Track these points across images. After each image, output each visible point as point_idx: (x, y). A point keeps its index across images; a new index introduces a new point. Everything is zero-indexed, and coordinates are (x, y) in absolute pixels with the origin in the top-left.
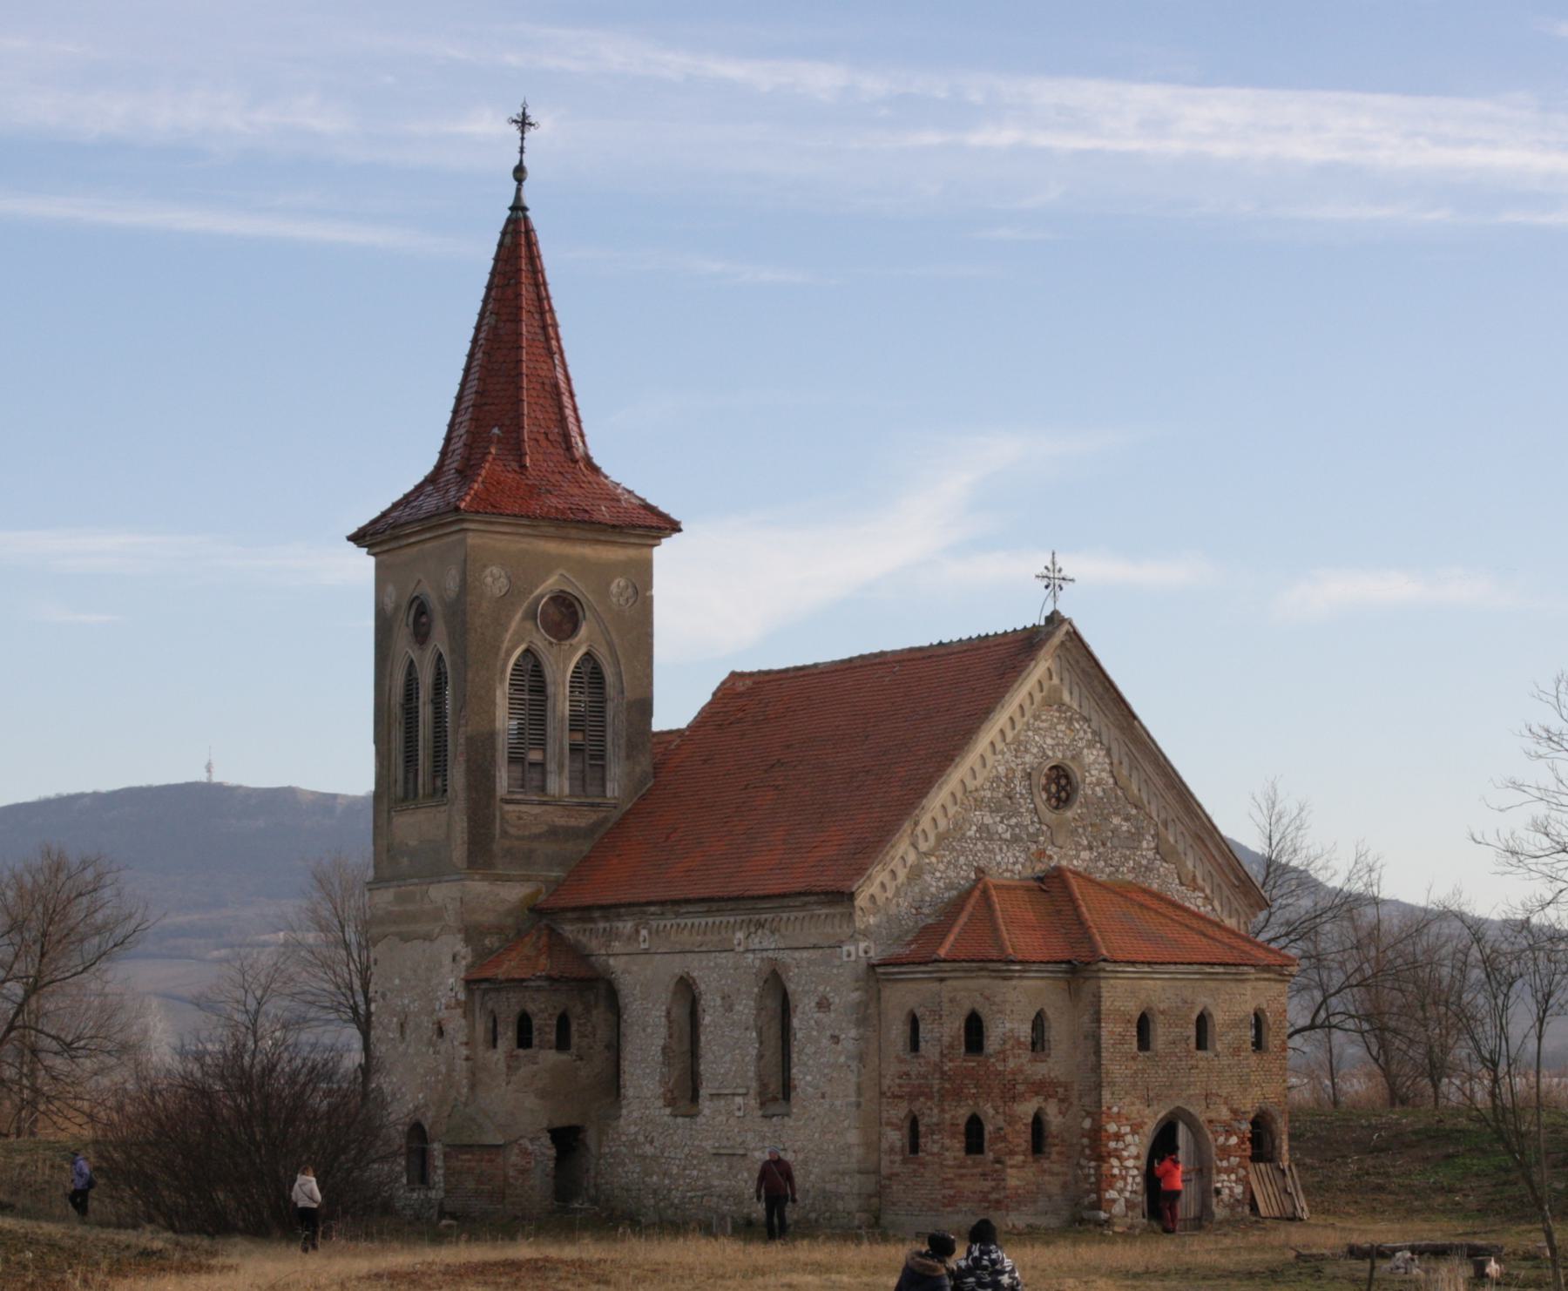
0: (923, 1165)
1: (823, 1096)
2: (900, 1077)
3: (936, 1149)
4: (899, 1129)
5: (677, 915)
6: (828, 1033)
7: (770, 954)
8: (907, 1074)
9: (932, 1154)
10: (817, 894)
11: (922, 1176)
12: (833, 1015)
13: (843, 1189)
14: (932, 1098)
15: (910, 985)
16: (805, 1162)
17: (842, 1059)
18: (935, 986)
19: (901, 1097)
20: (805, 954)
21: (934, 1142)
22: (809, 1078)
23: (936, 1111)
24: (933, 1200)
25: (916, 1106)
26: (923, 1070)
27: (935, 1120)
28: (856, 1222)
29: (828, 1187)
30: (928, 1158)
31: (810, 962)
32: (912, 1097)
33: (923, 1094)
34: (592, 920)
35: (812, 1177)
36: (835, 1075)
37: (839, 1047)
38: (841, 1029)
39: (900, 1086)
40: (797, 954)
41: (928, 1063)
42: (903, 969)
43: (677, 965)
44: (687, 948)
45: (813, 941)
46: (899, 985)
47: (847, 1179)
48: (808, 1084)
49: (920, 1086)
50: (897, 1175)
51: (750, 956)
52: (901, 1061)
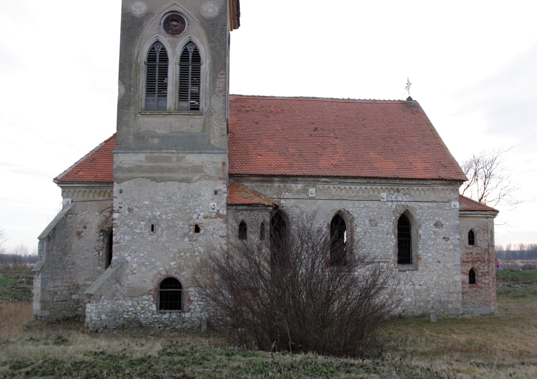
0: (481, 288)
1: (439, 262)
2: (468, 254)
3: (487, 282)
4: (467, 274)
5: (340, 183)
6: (442, 237)
7: (403, 203)
8: (471, 253)
9: (485, 284)
10: (443, 179)
11: (480, 292)
12: (444, 229)
13: (451, 299)
14: (484, 262)
15: (472, 219)
16: (427, 289)
17: (451, 247)
18: (485, 220)
19: (468, 262)
20: (426, 204)
21: (486, 279)
22: (430, 255)
23: (486, 267)
24: (485, 301)
25: (476, 266)
26: (479, 252)
27: (486, 271)
28: (461, 312)
29: (442, 299)
30: (483, 285)
31: (429, 208)
32: (473, 262)
33: (479, 261)
34: (272, 182)
35: (432, 295)
36: (446, 253)
37: (449, 242)
38: (451, 236)
39: (467, 258)
40: (421, 204)
41: (482, 249)
42: (473, 213)
43: (337, 206)
44: (345, 198)
45: (431, 199)
46: (467, 219)
47: (455, 295)
48: (430, 257)
49: (477, 258)
50: (467, 292)
51: (390, 203)
52: (467, 248)
